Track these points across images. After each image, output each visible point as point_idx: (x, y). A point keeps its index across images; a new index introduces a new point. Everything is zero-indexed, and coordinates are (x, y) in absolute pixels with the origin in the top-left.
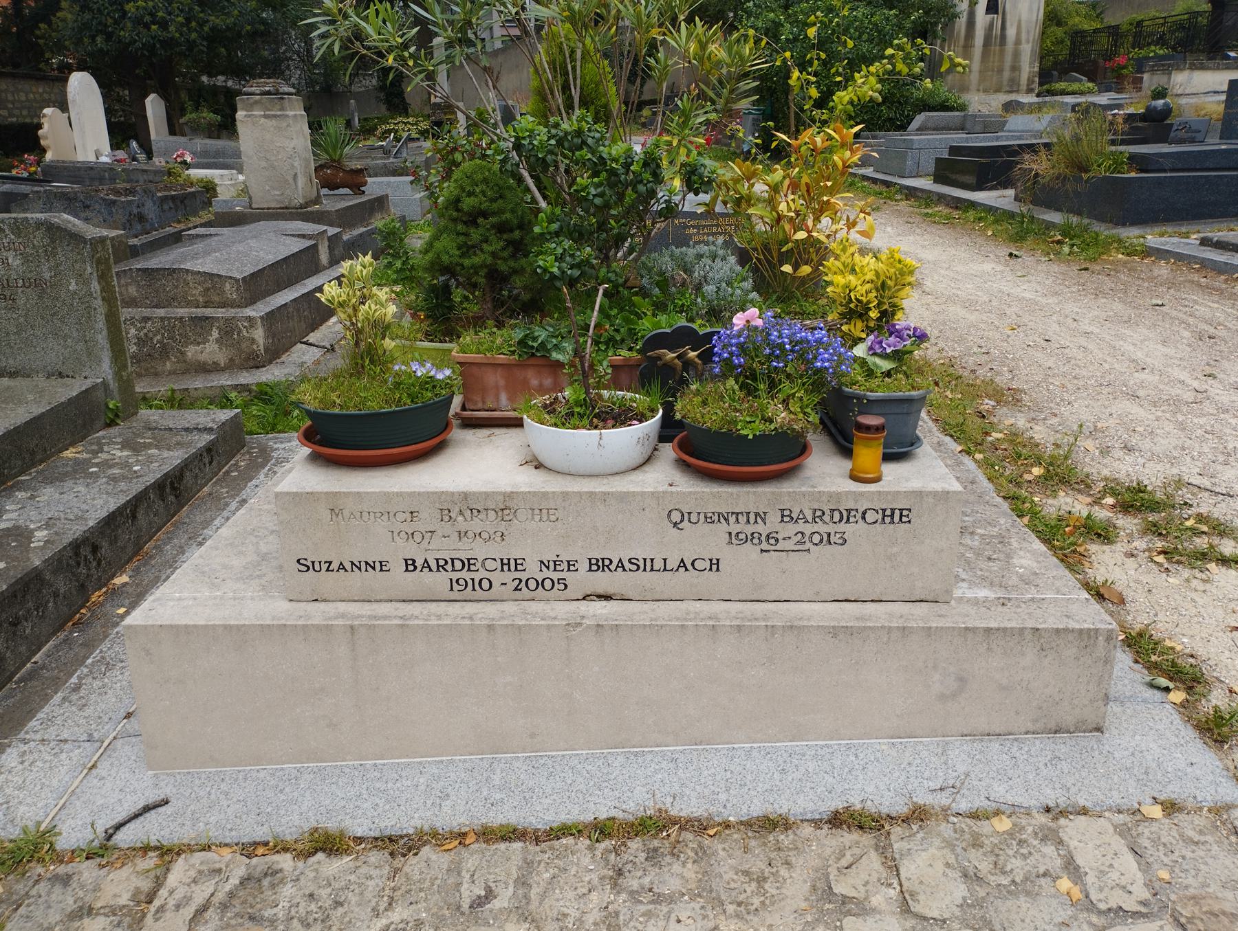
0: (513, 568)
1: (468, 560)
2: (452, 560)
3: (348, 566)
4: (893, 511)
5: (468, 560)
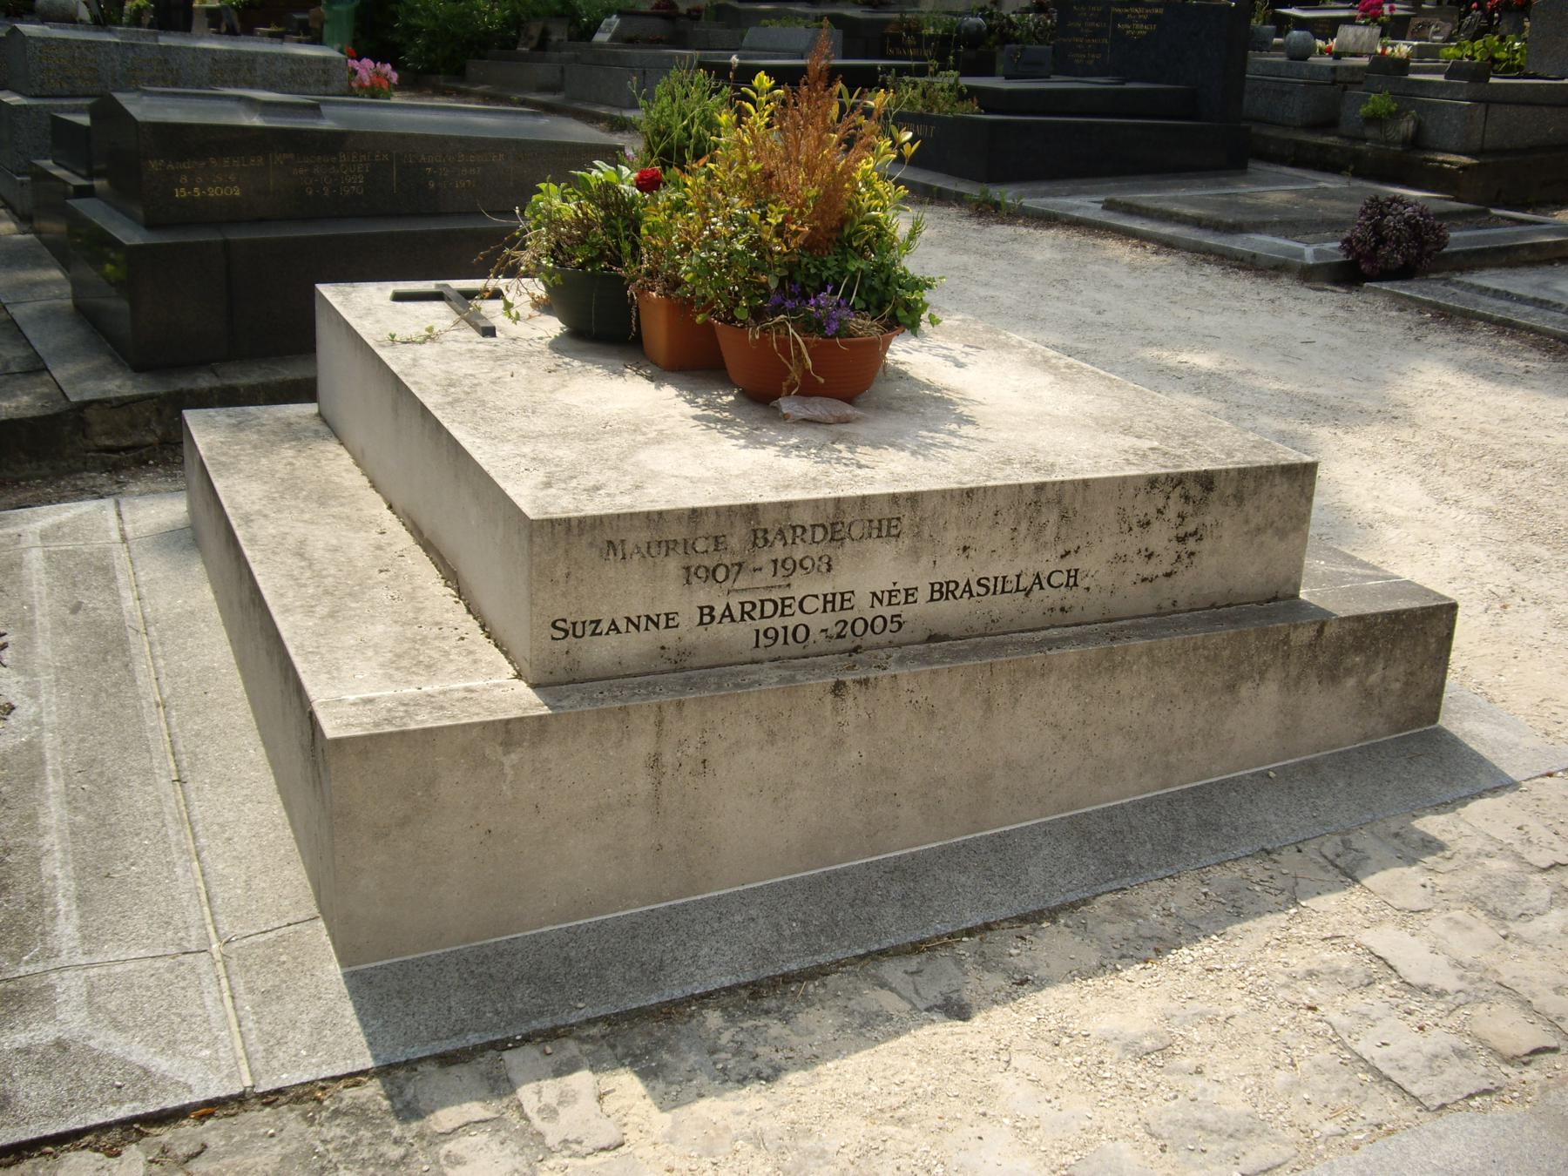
0: (838, 606)
1: (783, 600)
2: (762, 602)
3: (622, 625)
4: (742, 619)
5: (783, 600)
